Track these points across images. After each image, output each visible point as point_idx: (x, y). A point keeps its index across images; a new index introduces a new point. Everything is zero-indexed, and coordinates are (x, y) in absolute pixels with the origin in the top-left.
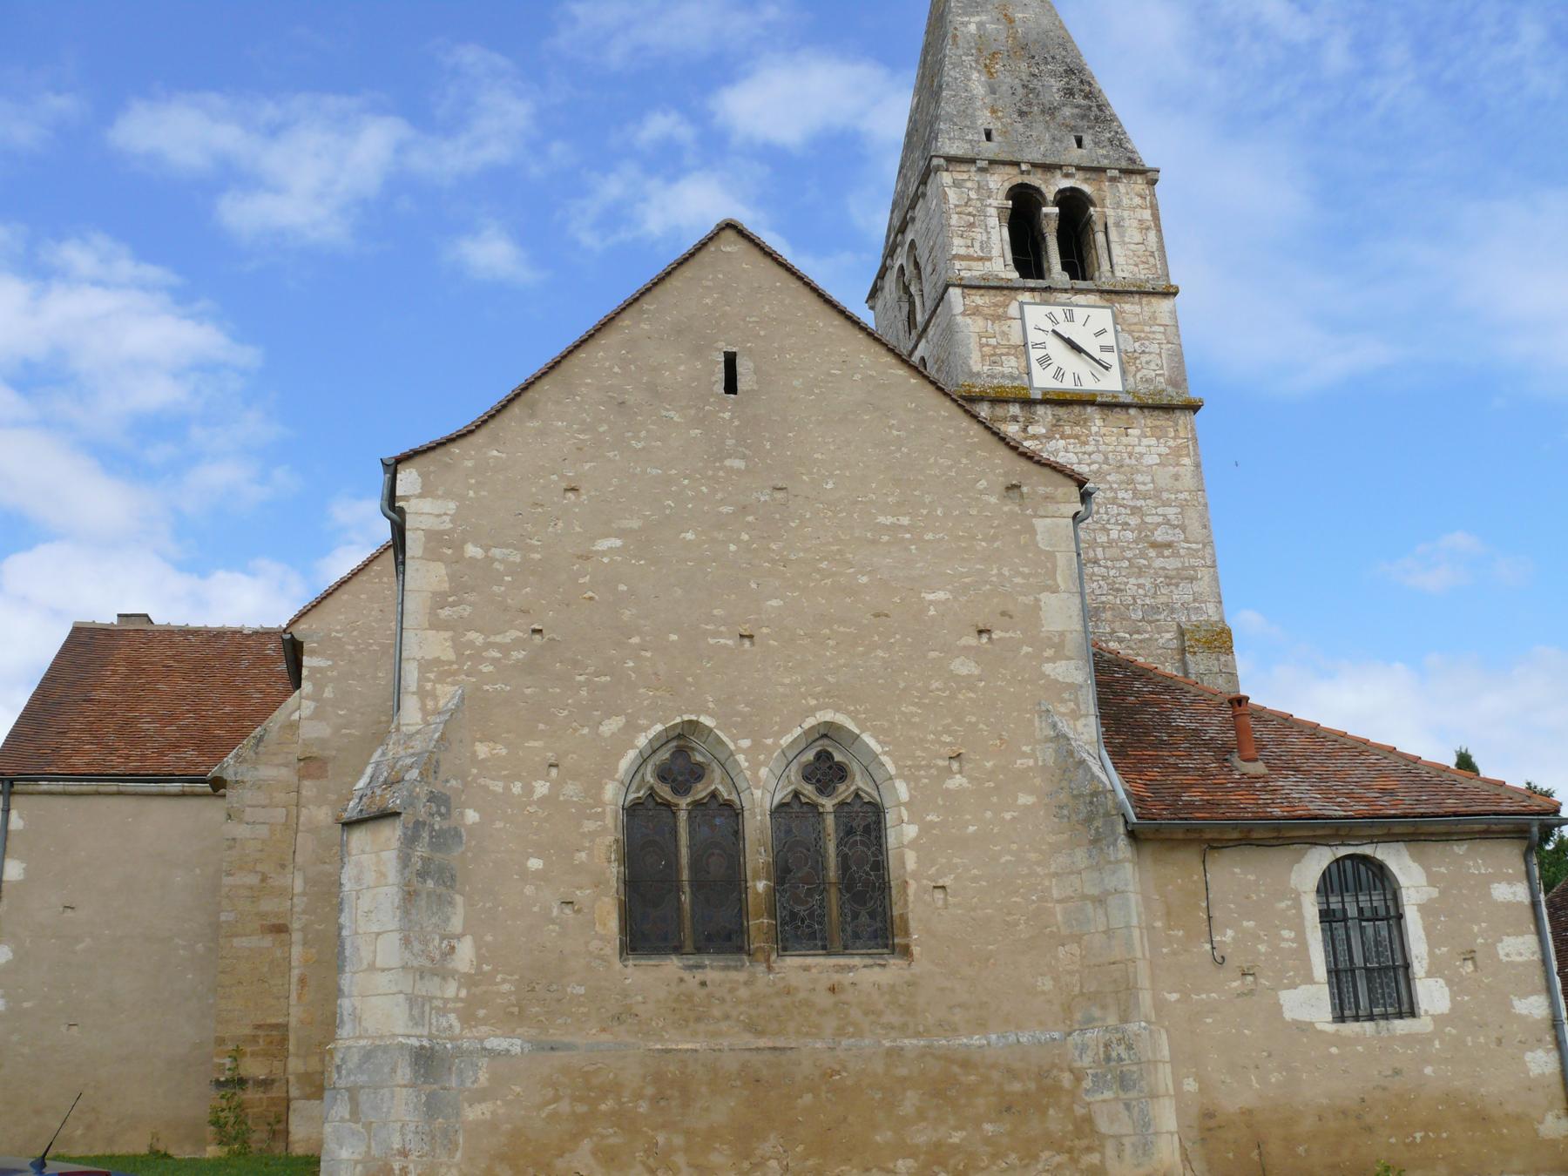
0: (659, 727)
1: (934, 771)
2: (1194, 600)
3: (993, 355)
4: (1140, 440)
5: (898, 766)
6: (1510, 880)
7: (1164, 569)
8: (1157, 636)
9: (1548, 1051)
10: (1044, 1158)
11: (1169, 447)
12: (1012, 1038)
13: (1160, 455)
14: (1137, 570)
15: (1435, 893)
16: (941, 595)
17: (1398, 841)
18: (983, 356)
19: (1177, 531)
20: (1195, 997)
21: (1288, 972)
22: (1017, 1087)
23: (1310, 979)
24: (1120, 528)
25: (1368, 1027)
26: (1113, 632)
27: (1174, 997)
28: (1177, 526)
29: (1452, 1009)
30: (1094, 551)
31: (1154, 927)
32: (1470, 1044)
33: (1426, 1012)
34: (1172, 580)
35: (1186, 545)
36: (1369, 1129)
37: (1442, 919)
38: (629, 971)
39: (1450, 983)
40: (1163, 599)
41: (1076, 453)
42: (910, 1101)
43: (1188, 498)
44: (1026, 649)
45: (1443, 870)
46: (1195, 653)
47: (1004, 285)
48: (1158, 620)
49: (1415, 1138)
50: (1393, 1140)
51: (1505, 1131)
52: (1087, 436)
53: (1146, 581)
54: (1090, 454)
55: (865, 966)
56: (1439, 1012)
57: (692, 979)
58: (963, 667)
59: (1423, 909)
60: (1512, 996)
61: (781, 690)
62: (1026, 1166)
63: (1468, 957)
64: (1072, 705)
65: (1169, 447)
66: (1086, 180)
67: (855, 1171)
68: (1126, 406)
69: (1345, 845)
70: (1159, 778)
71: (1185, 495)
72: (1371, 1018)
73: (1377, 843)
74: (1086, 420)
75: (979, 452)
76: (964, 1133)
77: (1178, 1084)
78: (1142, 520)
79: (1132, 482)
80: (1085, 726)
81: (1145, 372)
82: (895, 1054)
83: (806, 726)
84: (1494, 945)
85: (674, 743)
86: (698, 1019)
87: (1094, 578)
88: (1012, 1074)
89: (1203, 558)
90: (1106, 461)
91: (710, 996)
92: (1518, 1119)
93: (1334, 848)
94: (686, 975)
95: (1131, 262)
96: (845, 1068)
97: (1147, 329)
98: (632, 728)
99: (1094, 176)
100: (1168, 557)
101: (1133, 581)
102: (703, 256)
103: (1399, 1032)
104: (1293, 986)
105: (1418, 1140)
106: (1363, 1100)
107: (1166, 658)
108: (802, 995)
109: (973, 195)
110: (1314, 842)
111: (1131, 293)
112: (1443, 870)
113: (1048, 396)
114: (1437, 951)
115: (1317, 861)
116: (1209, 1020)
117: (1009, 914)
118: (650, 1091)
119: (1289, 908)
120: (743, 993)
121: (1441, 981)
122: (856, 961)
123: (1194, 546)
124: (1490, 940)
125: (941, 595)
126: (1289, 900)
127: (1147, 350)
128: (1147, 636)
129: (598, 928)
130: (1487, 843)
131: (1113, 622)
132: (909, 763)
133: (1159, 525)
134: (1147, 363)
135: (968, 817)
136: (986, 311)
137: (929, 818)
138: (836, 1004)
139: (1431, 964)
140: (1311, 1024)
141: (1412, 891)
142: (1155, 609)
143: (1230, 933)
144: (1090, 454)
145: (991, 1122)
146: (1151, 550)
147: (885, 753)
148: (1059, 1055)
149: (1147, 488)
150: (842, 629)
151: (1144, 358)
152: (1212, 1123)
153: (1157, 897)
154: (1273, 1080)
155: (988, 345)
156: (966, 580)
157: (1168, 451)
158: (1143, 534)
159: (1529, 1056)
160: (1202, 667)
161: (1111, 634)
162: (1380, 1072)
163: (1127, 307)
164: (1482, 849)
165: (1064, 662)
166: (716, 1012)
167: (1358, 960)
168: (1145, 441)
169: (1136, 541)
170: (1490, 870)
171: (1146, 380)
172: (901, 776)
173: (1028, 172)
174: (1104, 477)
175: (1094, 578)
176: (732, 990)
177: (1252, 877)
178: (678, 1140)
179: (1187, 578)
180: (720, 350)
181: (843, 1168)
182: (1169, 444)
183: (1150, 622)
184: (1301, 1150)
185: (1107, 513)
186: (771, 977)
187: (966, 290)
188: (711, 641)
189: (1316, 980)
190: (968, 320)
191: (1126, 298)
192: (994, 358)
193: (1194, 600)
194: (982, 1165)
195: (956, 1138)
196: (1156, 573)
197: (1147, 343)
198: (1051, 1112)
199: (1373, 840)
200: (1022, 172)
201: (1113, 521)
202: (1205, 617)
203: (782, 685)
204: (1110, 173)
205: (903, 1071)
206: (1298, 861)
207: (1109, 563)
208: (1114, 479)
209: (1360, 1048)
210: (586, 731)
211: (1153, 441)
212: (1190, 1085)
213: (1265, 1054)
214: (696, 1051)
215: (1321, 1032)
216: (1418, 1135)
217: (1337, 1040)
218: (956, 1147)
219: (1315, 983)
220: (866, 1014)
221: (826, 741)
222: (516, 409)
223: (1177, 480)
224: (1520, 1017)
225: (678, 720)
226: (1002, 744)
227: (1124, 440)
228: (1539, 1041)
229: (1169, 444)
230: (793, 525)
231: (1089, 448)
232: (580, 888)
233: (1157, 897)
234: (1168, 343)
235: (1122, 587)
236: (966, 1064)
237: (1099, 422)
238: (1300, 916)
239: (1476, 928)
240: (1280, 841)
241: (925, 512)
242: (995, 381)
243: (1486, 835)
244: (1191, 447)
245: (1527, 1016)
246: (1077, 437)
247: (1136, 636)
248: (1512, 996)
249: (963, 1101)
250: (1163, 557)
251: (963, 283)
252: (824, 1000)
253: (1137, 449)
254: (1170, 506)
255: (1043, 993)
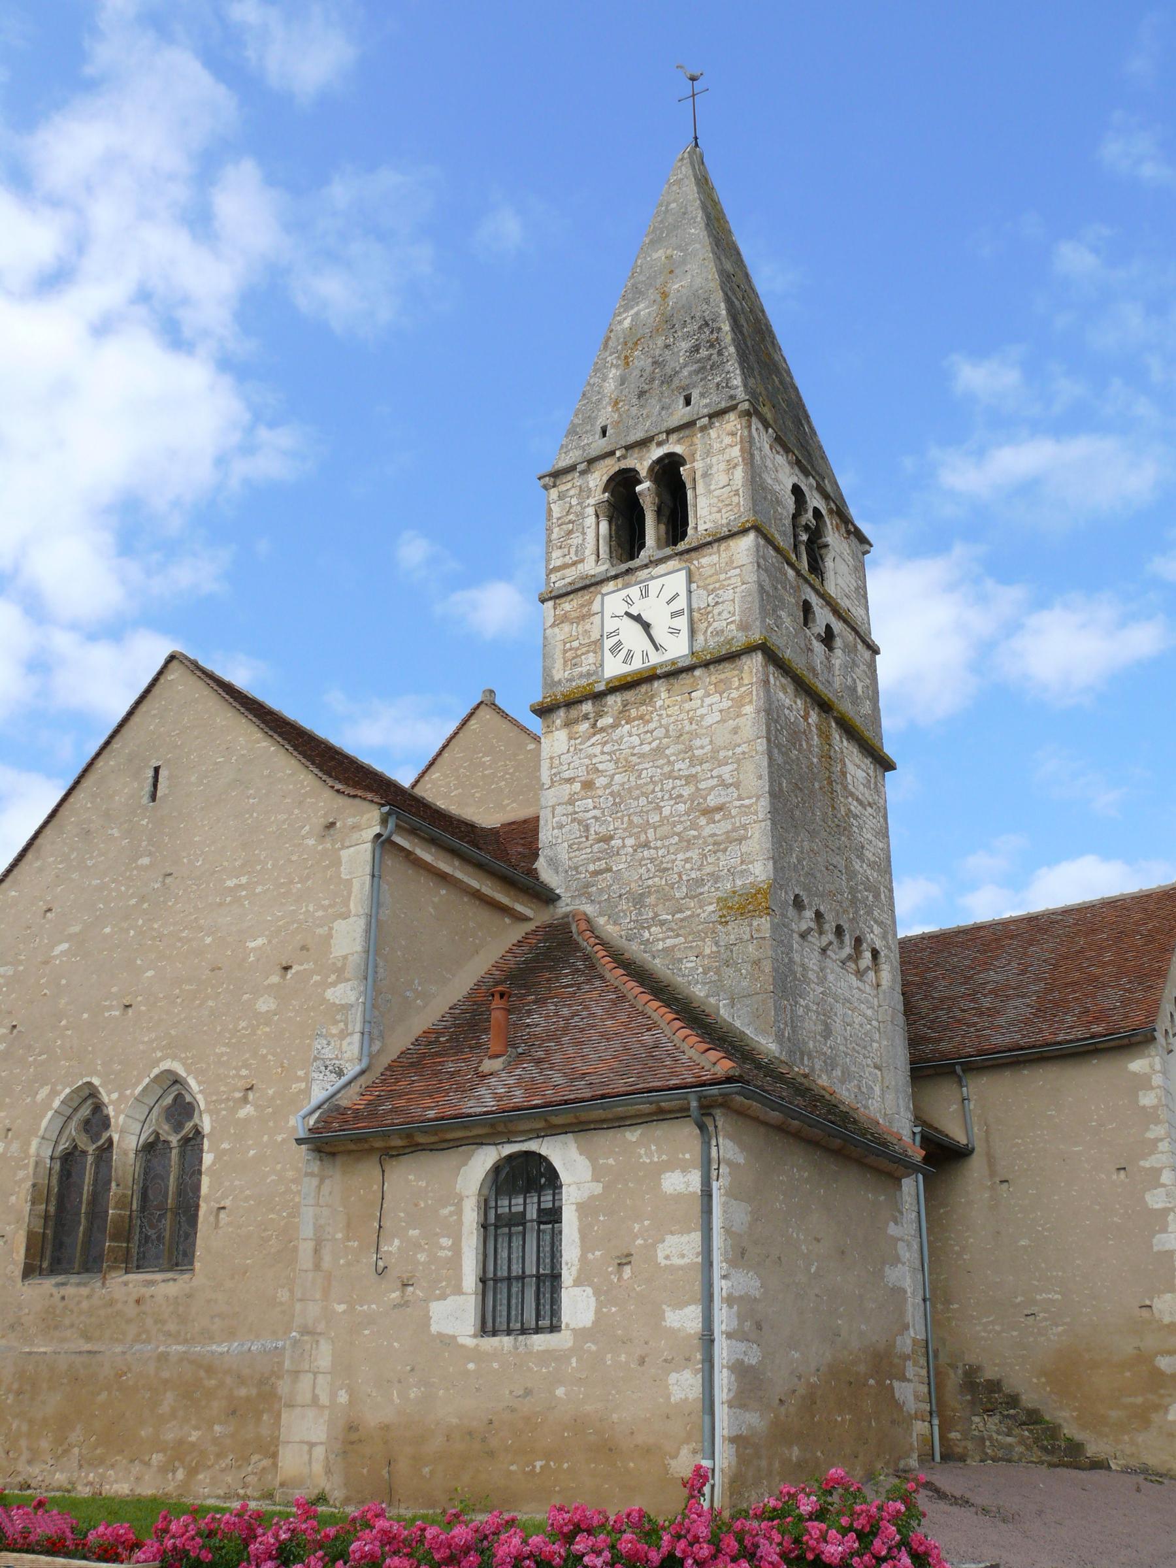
0: (68, 1090)
1: (231, 1103)
2: (742, 862)
3: (574, 658)
4: (703, 701)
5: (207, 1103)
6: (685, 1169)
7: (714, 835)
8: (699, 911)
9: (696, 1372)
10: (253, 1461)
11: (732, 699)
12: (246, 1347)
13: (721, 711)
14: (685, 844)
15: (598, 1188)
16: (260, 941)
17: (566, 1133)
18: (565, 662)
19: (732, 789)
20: (359, 1308)
21: (441, 1282)
22: (243, 1392)
23: (459, 1291)
24: (672, 802)
25: (506, 1341)
26: (656, 915)
27: (341, 1308)
28: (731, 785)
29: (596, 1322)
30: (646, 833)
31: (336, 1239)
32: (609, 1363)
33: (567, 1325)
34: (719, 846)
35: (738, 803)
36: (491, 1454)
37: (601, 1218)
38: (25, 1288)
39: (597, 1293)
40: (708, 869)
41: (638, 735)
42: (169, 1400)
43: (746, 750)
44: (316, 978)
45: (611, 1161)
46: (727, 922)
47: (588, 582)
48: (702, 894)
49: (534, 1467)
50: (513, 1468)
51: (632, 1465)
52: (652, 713)
53: (694, 854)
54: (652, 732)
55: (164, 1281)
56: (581, 1325)
57: (57, 1293)
58: (265, 1004)
59: (583, 1208)
60: (664, 1307)
61: (141, 1047)
62: (239, 1467)
63: (624, 1261)
64: (342, 1025)
65: (732, 699)
66: (679, 441)
67: (124, 1461)
68: (690, 669)
69: (512, 1142)
70: (683, 1069)
71: (744, 747)
72: (509, 1332)
73: (543, 1137)
74: (652, 697)
75: (308, 800)
76: (200, 1433)
77: (333, 1395)
78: (697, 788)
79: (691, 748)
80: (349, 1044)
81: (715, 625)
82: (163, 1358)
83: (152, 1076)
84: (654, 1246)
85: (89, 1102)
86: (56, 1328)
87: (643, 863)
88: (241, 1380)
89: (756, 813)
90: (667, 736)
91: (65, 1308)
92: (647, 1451)
93: (500, 1147)
94: (54, 1291)
95: (715, 509)
96: (130, 1370)
97: (723, 577)
98: (54, 1093)
99: (687, 432)
100: (719, 821)
101: (681, 856)
102: (156, 691)
103: (536, 1348)
104: (443, 1297)
105: (538, 1470)
106: (491, 1422)
107: (706, 934)
108: (119, 1306)
109: (574, 501)
110: (479, 1141)
111: (710, 543)
112: (611, 1161)
113: (611, 685)
114: (590, 1256)
115: (485, 1159)
116: (367, 1332)
117: (265, 1230)
118: (15, 1386)
119: (451, 1214)
120: (85, 1305)
121: (589, 1290)
122: (159, 1277)
123: (747, 802)
124: (650, 1241)
125: (260, 941)
126: (451, 1205)
127: (720, 600)
128: (689, 913)
129: (14, 1255)
130: (665, 1125)
131: (657, 905)
132: (214, 1098)
133: (713, 788)
134: (719, 614)
135: (251, 1142)
136: (574, 615)
137: (223, 1146)
138: (139, 1315)
139: (580, 1271)
140: (454, 1337)
141: (573, 1189)
142: (700, 882)
143: (397, 1242)
144: (652, 732)
145: (220, 1423)
146: (702, 818)
147: (200, 1091)
148: (278, 1363)
149: (705, 751)
150: (187, 987)
151: (720, 608)
152: (354, 1436)
153: (341, 1209)
154: (412, 1396)
155: (571, 649)
156: (280, 923)
157: (730, 703)
158: (696, 802)
159: (673, 1377)
160: (732, 937)
161: (653, 918)
162: (511, 1392)
163: (704, 561)
164: (658, 1133)
165: (343, 984)
166: (67, 1322)
167: (531, 1269)
168: (708, 701)
169: (687, 813)
170: (664, 1157)
171: (717, 633)
172: (209, 1111)
173: (624, 457)
174: (664, 752)
175: (643, 863)
176: (79, 1303)
177: (423, 1184)
178: (25, 1428)
179: (736, 840)
180: (150, 767)
181: (117, 1458)
182: (732, 695)
183: (693, 897)
184: (426, 1470)
185: (662, 790)
186: (104, 1291)
187: (557, 601)
188: (107, 1014)
189: (464, 1290)
190: (556, 630)
191: (706, 551)
192: (572, 661)
193: (742, 862)
194: (209, 1463)
195: (194, 1436)
196: (705, 843)
197: (720, 592)
198: (265, 1417)
199: (539, 1135)
200: (619, 459)
201: (666, 797)
202: (751, 879)
203: (143, 1043)
204: (699, 424)
205: (166, 1374)
206: (465, 1164)
207: (659, 843)
208: (672, 751)
209: (495, 1365)
210: (29, 1100)
211: (717, 697)
212: (343, 1397)
213: (408, 1368)
214: (45, 1353)
215: (463, 1346)
216: (538, 1464)
217: (476, 1355)
218: (193, 1445)
219: (463, 1294)
220: (156, 1322)
221: (177, 1086)
222: (30, 856)
223: (736, 733)
224: (672, 1332)
225: (80, 1083)
226: (282, 1071)
227: (687, 706)
228: (688, 1360)
229: (732, 695)
230: (170, 904)
231: (652, 726)
232: (9, 1224)
233: (341, 1209)
234: (743, 584)
235: (669, 865)
236: (210, 1370)
237: (664, 695)
238: (460, 1222)
239: (637, 1227)
240: (445, 1145)
241: (259, 867)
242: (574, 684)
243: (660, 1115)
244: (754, 693)
245: (679, 1330)
246: (641, 718)
247: (678, 916)
248: (664, 1307)
249: (203, 1403)
250: (714, 822)
251: (553, 594)
252: (131, 1310)
253: (699, 712)
254: (727, 764)
255: (281, 1304)
